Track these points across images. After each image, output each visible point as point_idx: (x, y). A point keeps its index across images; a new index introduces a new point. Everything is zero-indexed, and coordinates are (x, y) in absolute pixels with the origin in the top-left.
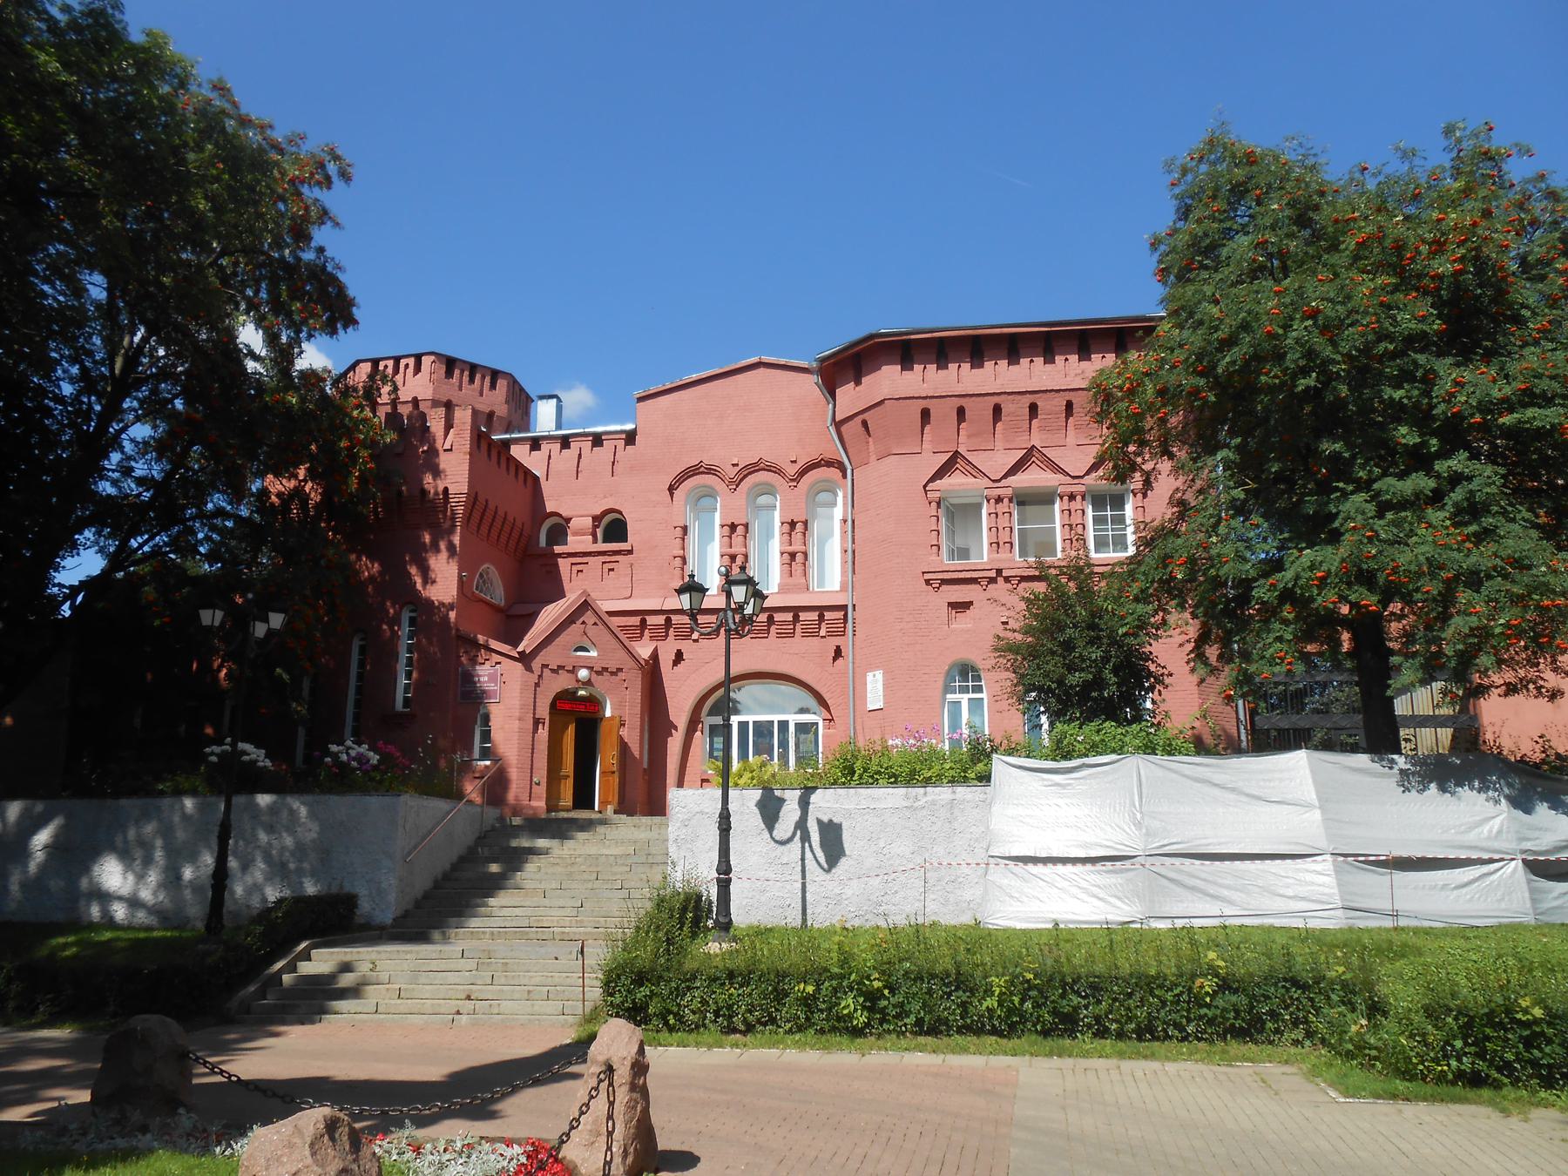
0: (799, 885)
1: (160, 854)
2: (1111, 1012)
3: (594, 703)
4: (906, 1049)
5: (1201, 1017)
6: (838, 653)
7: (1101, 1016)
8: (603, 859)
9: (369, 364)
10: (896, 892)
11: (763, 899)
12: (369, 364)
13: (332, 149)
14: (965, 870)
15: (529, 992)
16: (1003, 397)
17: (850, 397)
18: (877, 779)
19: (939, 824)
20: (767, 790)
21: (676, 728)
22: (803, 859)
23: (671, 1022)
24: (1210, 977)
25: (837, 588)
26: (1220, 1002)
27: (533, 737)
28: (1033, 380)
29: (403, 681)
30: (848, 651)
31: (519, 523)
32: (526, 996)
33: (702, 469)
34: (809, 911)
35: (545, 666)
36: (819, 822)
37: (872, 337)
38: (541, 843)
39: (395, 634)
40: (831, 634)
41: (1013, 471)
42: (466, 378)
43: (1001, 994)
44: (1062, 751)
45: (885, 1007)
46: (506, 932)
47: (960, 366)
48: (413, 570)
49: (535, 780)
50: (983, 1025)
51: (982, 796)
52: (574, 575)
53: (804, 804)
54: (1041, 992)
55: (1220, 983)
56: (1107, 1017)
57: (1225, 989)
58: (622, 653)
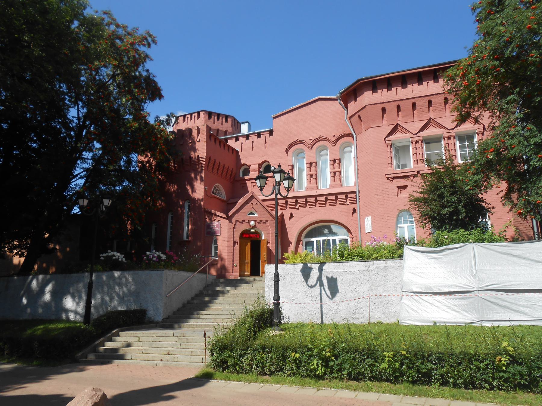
0: (319, 305)
1: (84, 294)
2: (449, 373)
3: (257, 234)
4: (341, 388)
5: (501, 378)
6: (354, 211)
7: (444, 375)
8: (249, 295)
9: (182, 117)
10: (362, 308)
11: (304, 311)
12: (182, 117)
13: (148, 32)
14: (392, 298)
15: (192, 352)
16: (416, 99)
17: (353, 107)
18: (354, 259)
19: (380, 277)
20: (305, 264)
21: (291, 244)
22: (321, 294)
23: (237, 369)
24: (505, 356)
25: (353, 185)
26: (511, 369)
27: (233, 248)
28: (429, 90)
29: (186, 229)
30: (357, 210)
31: (230, 168)
32: (190, 354)
33: (298, 142)
34: (324, 317)
35: (237, 221)
36: (327, 277)
37: (359, 80)
38: (228, 288)
39: (183, 212)
40: (351, 203)
41: (422, 129)
42: (216, 119)
43: (389, 361)
44: (438, 243)
45: (333, 366)
46: (202, 325)
47: (397, 88)
48: (188, 187)
49: (235, 264)
50: (382, 377)
51: (399, 265)
52: (252, 187)
53: (321, 270)
54: (410, 360)
55: (511, 359)
56: (447, 375)
57: (514, 363)
58: (268, 215)
